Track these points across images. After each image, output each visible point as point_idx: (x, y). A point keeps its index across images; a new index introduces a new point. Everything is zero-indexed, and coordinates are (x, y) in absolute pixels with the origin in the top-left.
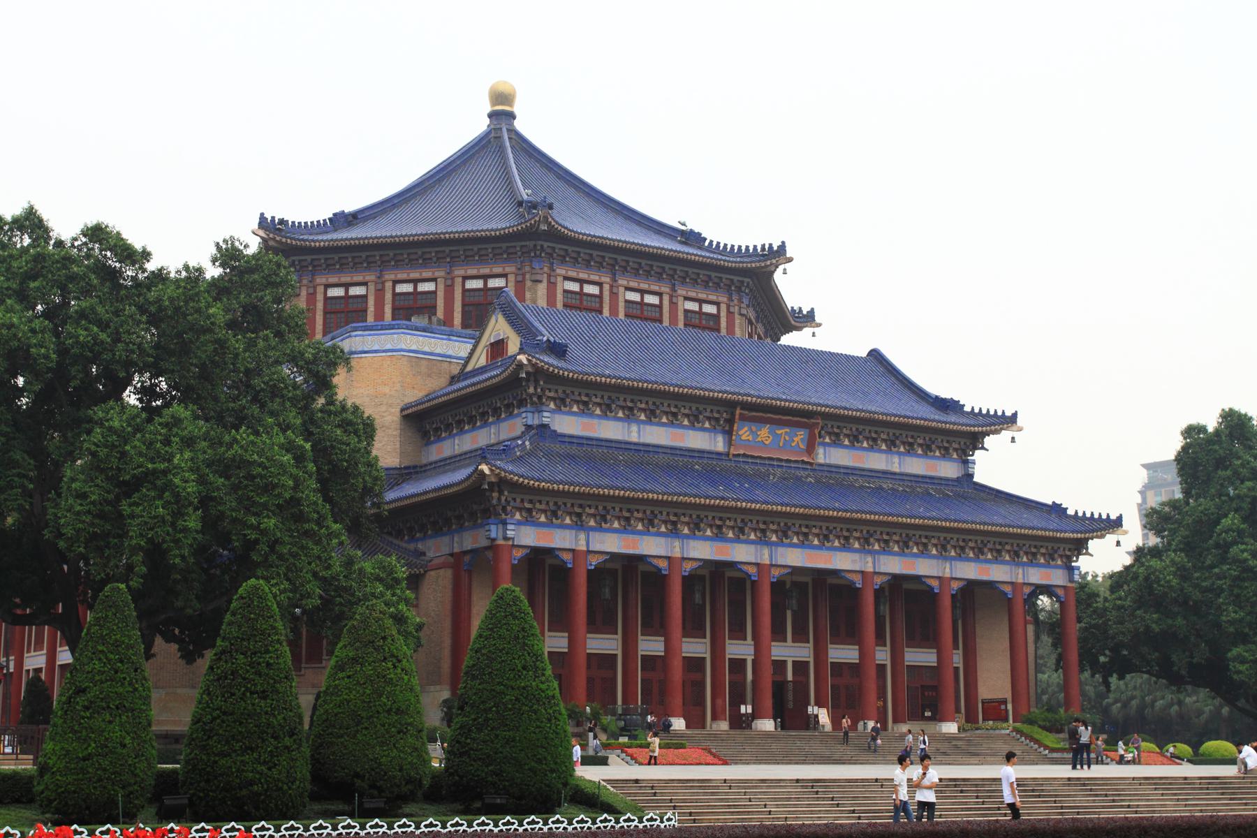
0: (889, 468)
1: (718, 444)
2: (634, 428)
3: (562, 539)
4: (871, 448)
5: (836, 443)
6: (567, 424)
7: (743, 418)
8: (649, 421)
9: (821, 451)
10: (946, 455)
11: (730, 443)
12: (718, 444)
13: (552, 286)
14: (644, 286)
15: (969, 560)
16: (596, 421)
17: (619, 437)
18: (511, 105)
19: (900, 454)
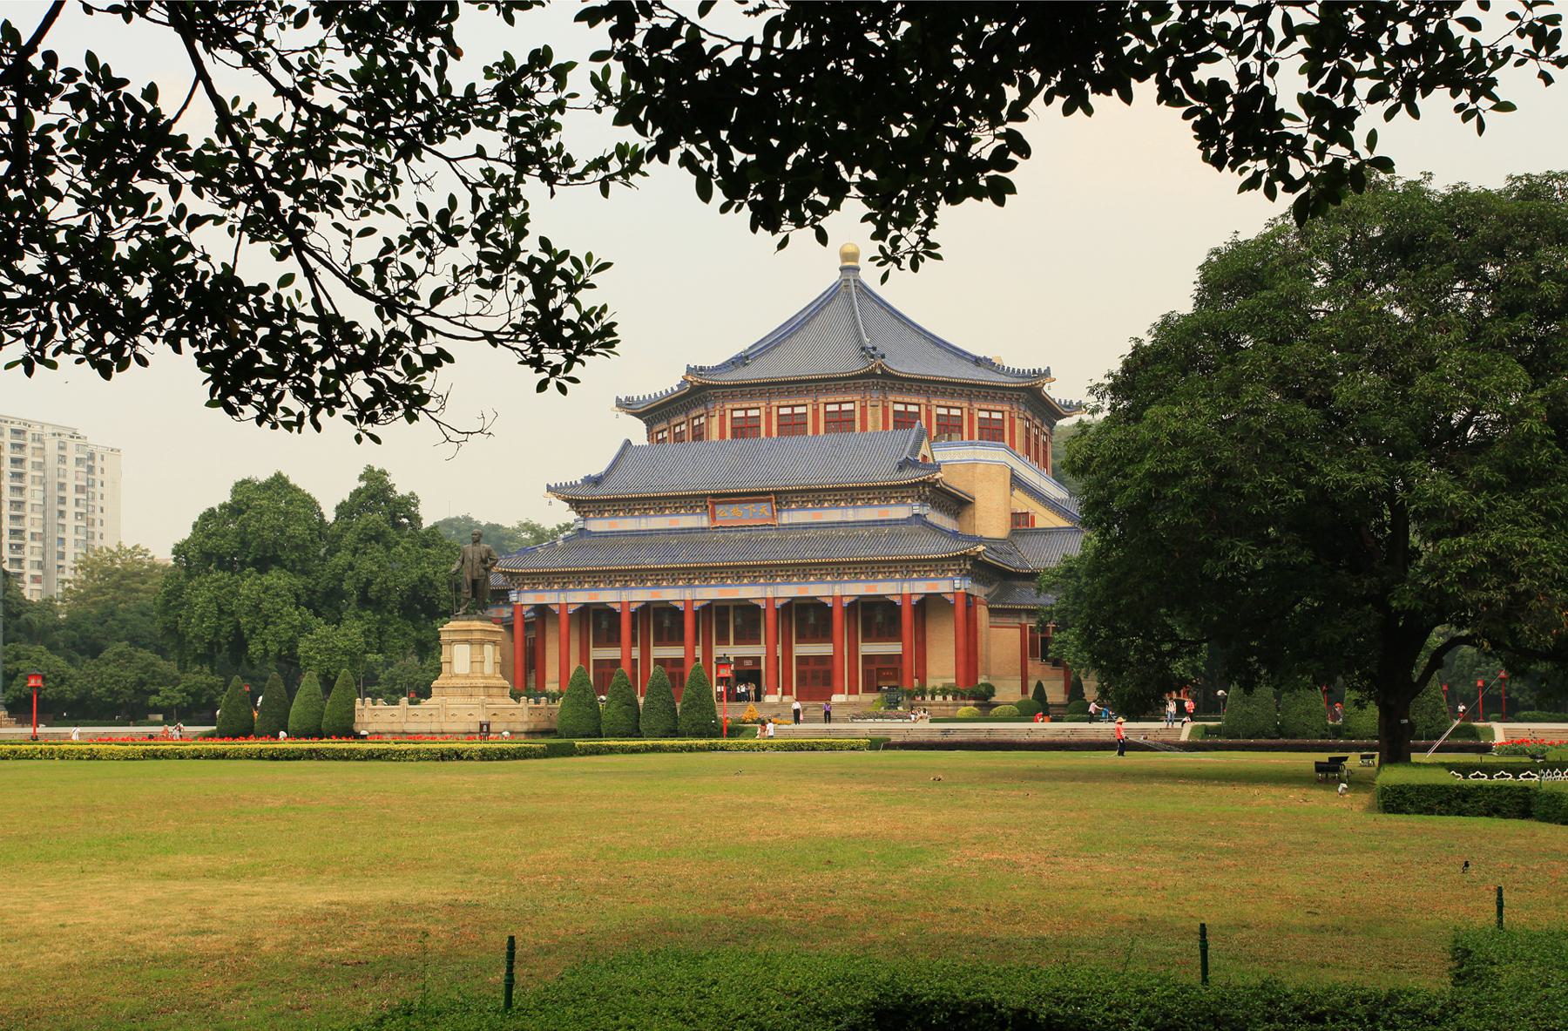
0: (845, 519)
1: (704, 521)
2: (643, 520)
3: (549, 598)
4: (830, 508)
5: (802, 508)
6: (598, 525)
7: (714, 504)
8: (655, 516)
9: (785, 515)
10: (902, 502)
11: (714, 519)
12: (704, 521)
13: (722, 417)
14: (792, 402)
15: (858, 580)
16: (617, 520)
17: (634, 528)
18: (856, 260)
19: (855, 507)
